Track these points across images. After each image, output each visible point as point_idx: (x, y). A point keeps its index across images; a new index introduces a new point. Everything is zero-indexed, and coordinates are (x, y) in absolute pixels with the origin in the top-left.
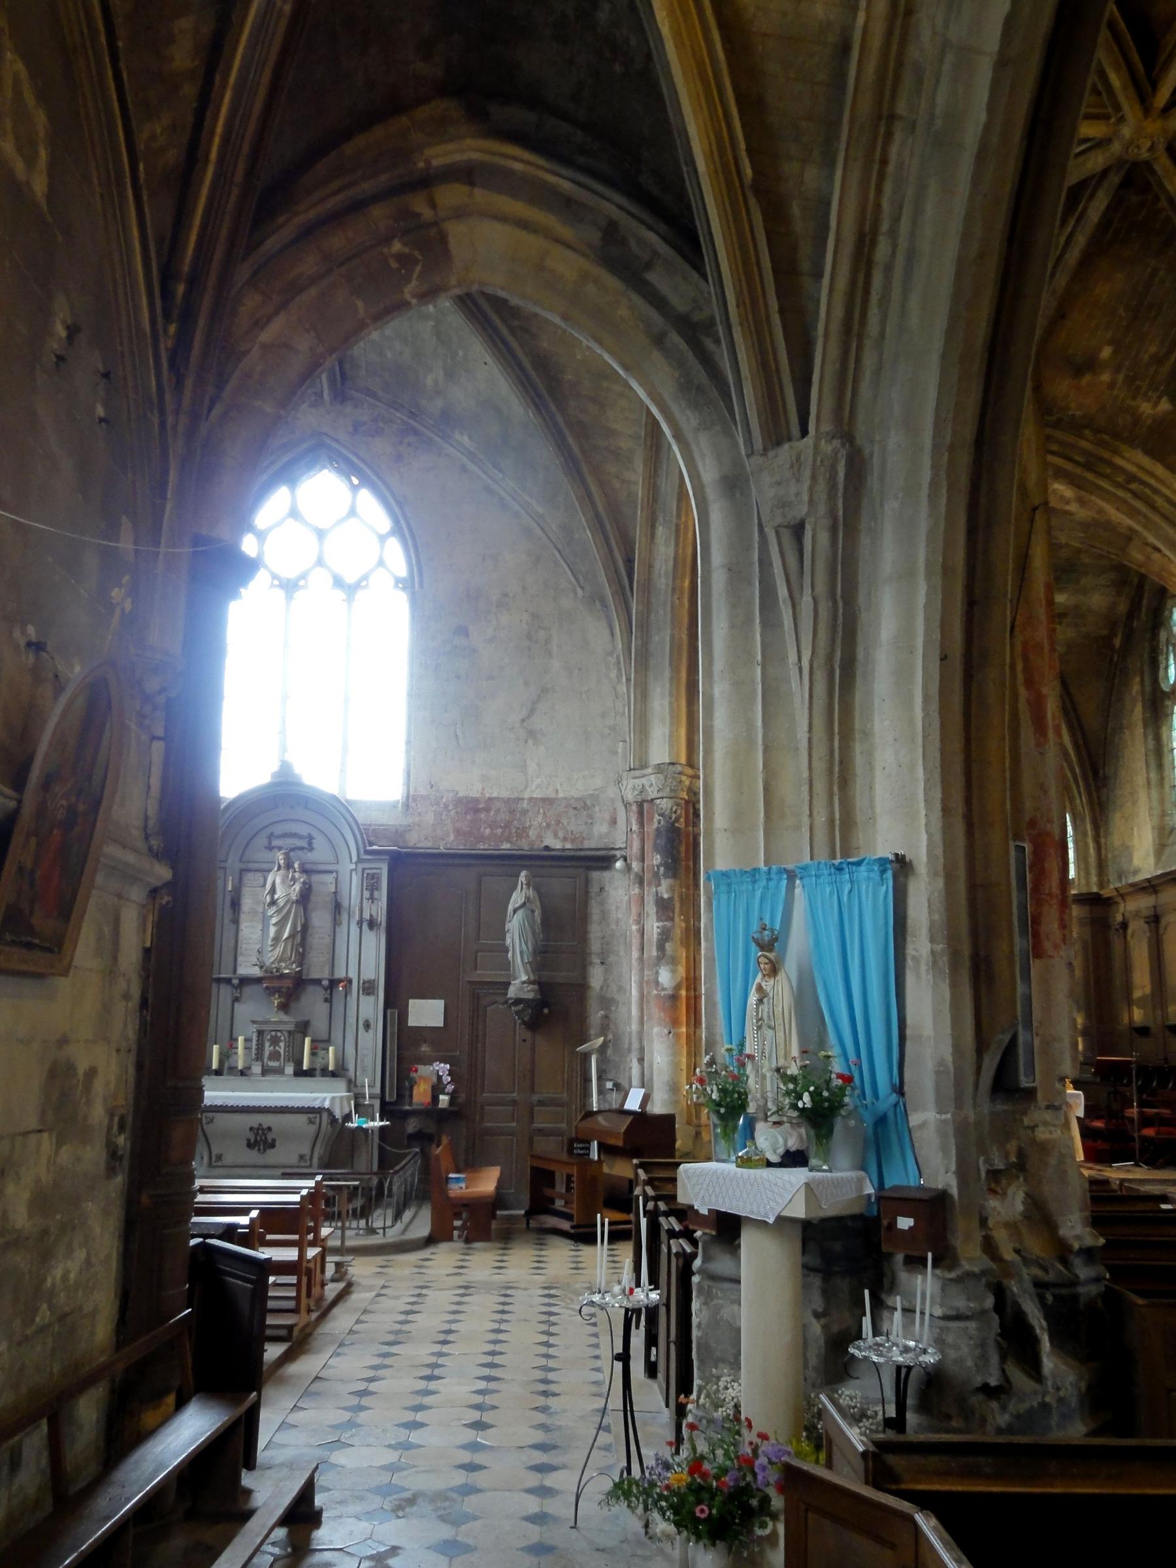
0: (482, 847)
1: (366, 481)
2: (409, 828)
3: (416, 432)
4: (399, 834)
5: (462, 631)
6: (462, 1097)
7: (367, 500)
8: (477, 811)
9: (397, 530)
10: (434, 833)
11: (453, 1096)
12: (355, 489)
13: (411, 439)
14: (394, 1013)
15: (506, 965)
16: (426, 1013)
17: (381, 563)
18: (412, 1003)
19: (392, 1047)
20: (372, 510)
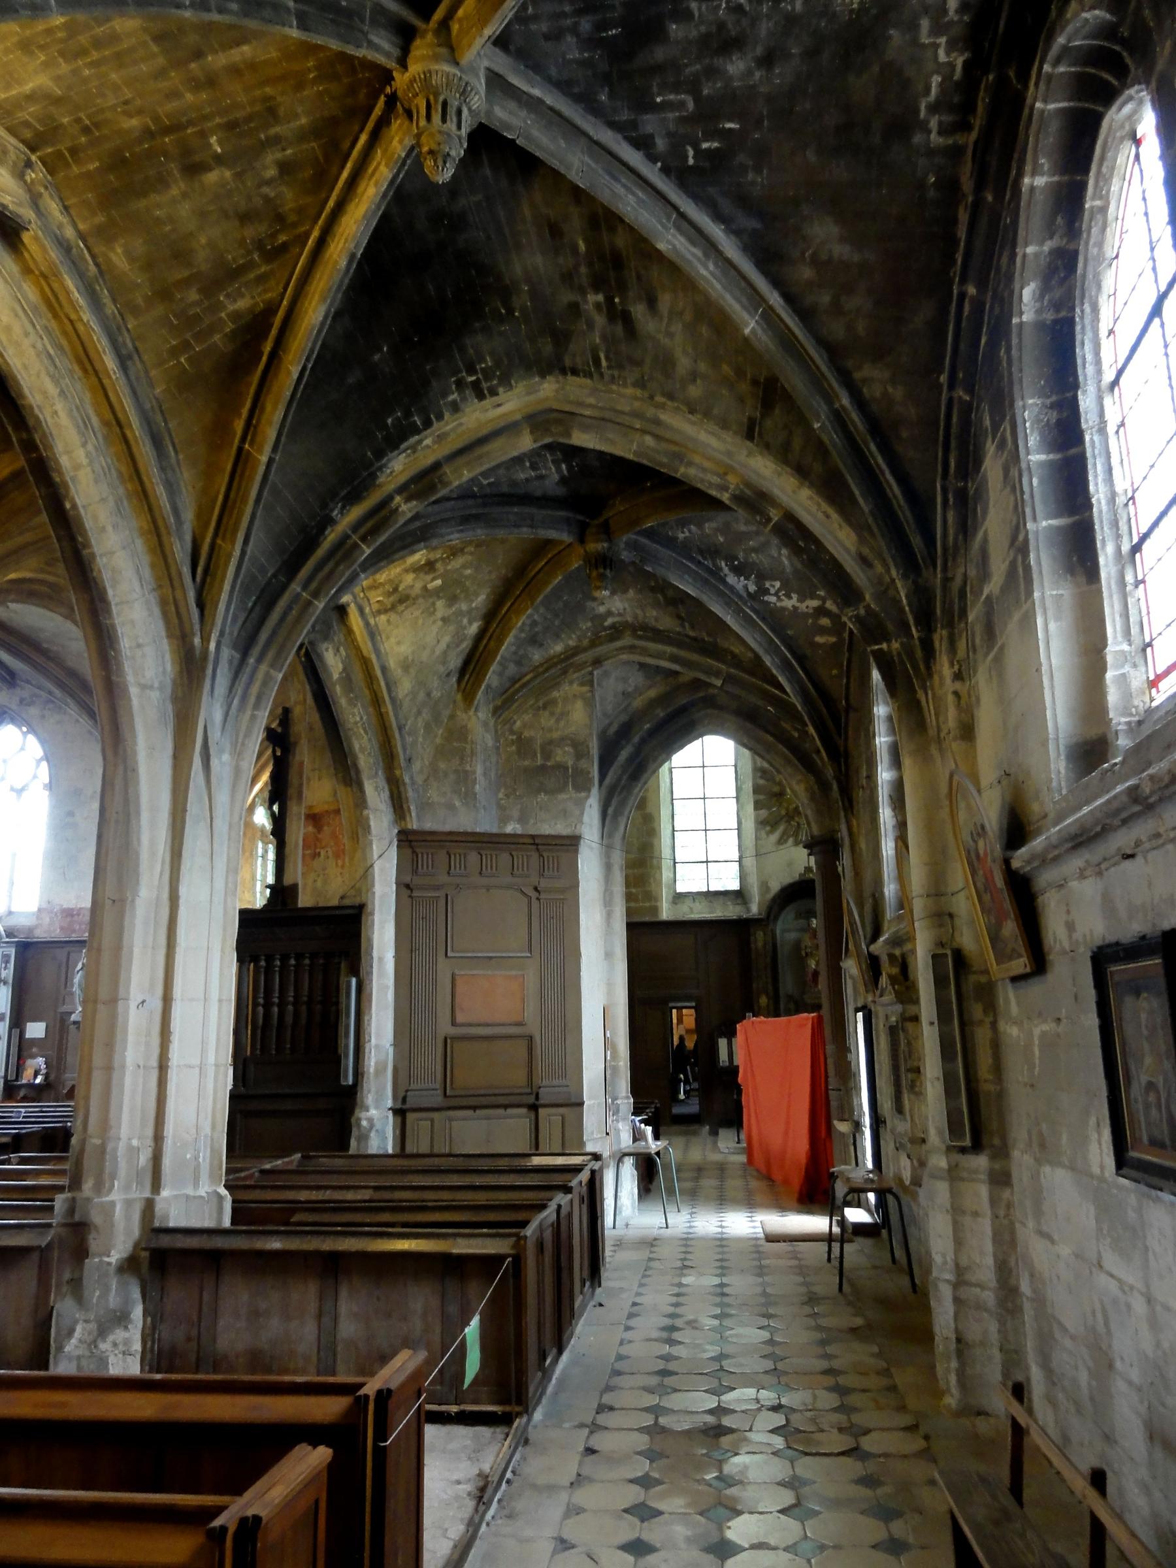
0: (74, 937)
1: (32, 730)
2: (36, 927)
3: (53, 702)
4: (31, 930)
5: (71, 814)
6: (52, 1077)
7: (32, 740)
8: (72, 916)
9: (46, 758)
10: (49, 930)
11: (47, 1076)
12: (25, 734)
13: (51, 706)
14: (16, 1032)
15: (73, 1003)
16: (36, 1030)
17: (35, 777)
18: (28, 1024)
19: (14, 1050)
20: (34, 747)
